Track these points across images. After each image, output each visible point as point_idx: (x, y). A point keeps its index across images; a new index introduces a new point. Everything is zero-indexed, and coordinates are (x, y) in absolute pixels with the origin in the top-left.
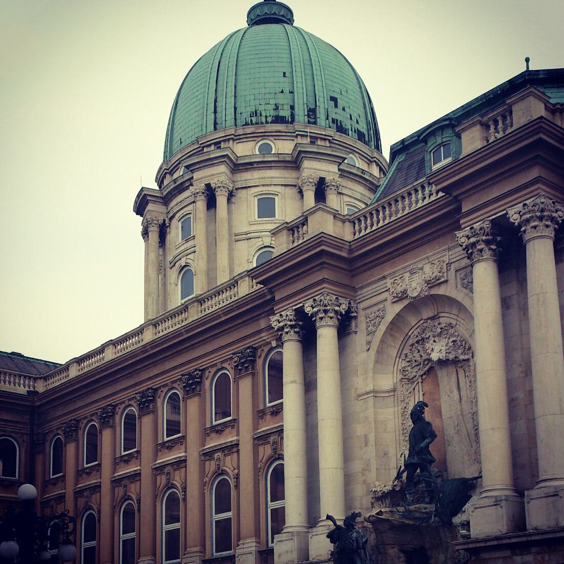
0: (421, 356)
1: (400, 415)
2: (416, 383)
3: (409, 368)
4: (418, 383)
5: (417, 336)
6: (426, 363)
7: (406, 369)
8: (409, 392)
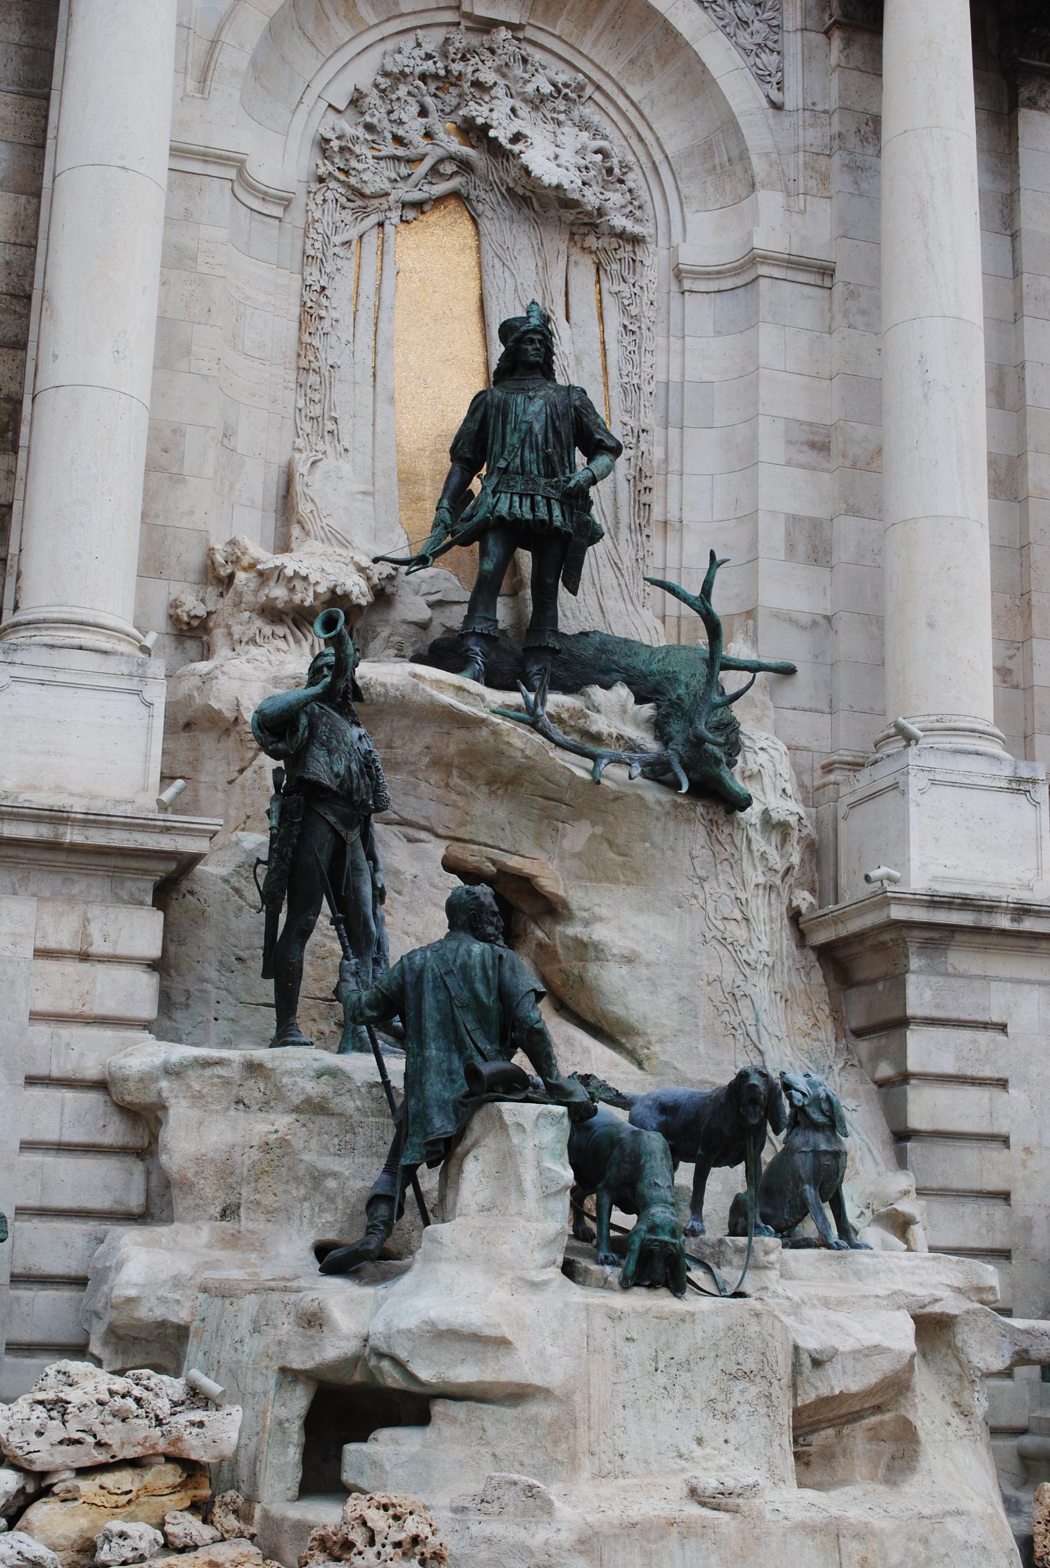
0: (428, 135)
1: (296, 310)
2: (374, 219)
3: (370, 154)
4: (381, 225)
5: (429, 57)
6: (449, 168)
7: (357, 149)
8: (345, 237)
